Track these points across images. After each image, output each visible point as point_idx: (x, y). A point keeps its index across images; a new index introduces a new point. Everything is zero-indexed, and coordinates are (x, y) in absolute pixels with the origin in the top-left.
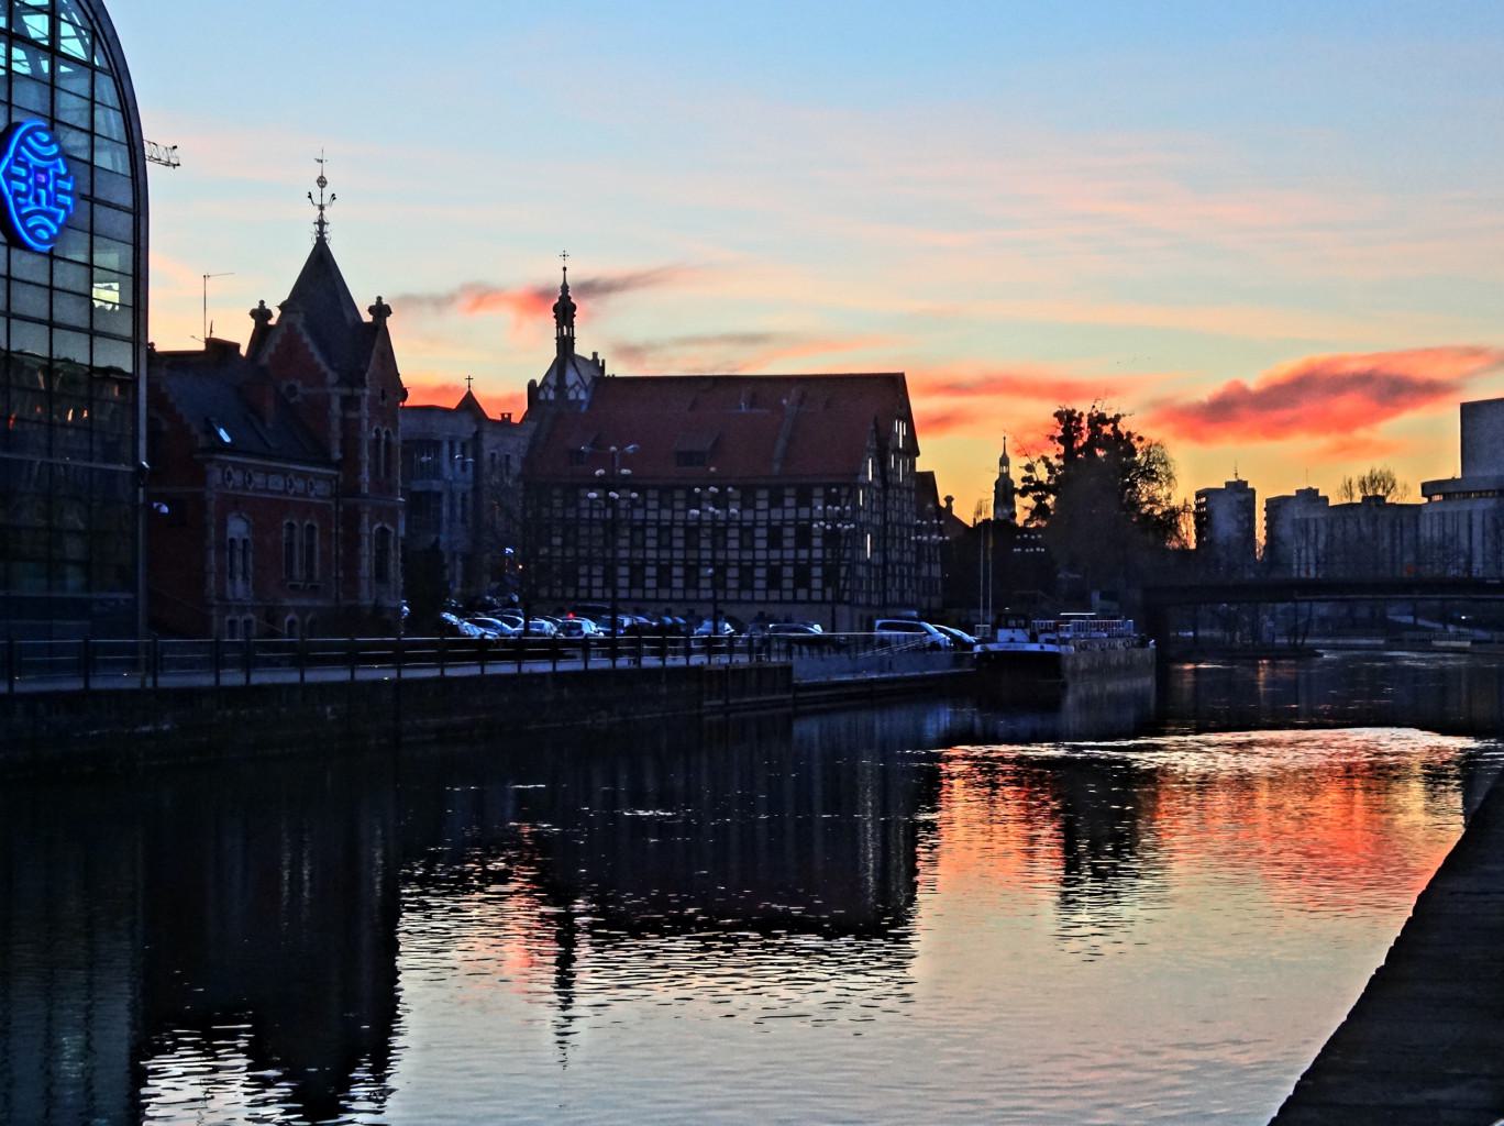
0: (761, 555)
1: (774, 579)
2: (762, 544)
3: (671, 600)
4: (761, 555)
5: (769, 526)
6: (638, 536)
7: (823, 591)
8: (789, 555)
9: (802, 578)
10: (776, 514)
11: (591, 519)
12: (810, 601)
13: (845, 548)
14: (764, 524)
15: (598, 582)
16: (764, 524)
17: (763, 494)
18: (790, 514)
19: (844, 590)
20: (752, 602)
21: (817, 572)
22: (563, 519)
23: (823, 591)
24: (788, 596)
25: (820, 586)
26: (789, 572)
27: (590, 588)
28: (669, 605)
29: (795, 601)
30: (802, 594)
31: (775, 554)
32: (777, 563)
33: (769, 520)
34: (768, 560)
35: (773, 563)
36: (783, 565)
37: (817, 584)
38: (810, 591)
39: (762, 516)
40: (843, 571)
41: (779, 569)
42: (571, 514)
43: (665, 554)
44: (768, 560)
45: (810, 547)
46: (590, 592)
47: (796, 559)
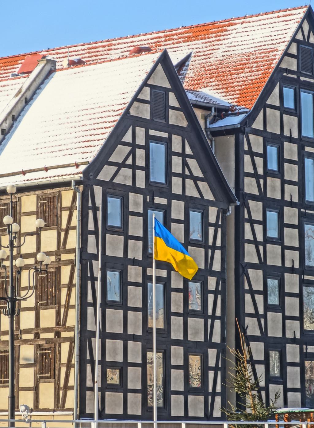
7: (36, 389)
13: (68, 306)
19: (67, 388)
25: (31, 384)
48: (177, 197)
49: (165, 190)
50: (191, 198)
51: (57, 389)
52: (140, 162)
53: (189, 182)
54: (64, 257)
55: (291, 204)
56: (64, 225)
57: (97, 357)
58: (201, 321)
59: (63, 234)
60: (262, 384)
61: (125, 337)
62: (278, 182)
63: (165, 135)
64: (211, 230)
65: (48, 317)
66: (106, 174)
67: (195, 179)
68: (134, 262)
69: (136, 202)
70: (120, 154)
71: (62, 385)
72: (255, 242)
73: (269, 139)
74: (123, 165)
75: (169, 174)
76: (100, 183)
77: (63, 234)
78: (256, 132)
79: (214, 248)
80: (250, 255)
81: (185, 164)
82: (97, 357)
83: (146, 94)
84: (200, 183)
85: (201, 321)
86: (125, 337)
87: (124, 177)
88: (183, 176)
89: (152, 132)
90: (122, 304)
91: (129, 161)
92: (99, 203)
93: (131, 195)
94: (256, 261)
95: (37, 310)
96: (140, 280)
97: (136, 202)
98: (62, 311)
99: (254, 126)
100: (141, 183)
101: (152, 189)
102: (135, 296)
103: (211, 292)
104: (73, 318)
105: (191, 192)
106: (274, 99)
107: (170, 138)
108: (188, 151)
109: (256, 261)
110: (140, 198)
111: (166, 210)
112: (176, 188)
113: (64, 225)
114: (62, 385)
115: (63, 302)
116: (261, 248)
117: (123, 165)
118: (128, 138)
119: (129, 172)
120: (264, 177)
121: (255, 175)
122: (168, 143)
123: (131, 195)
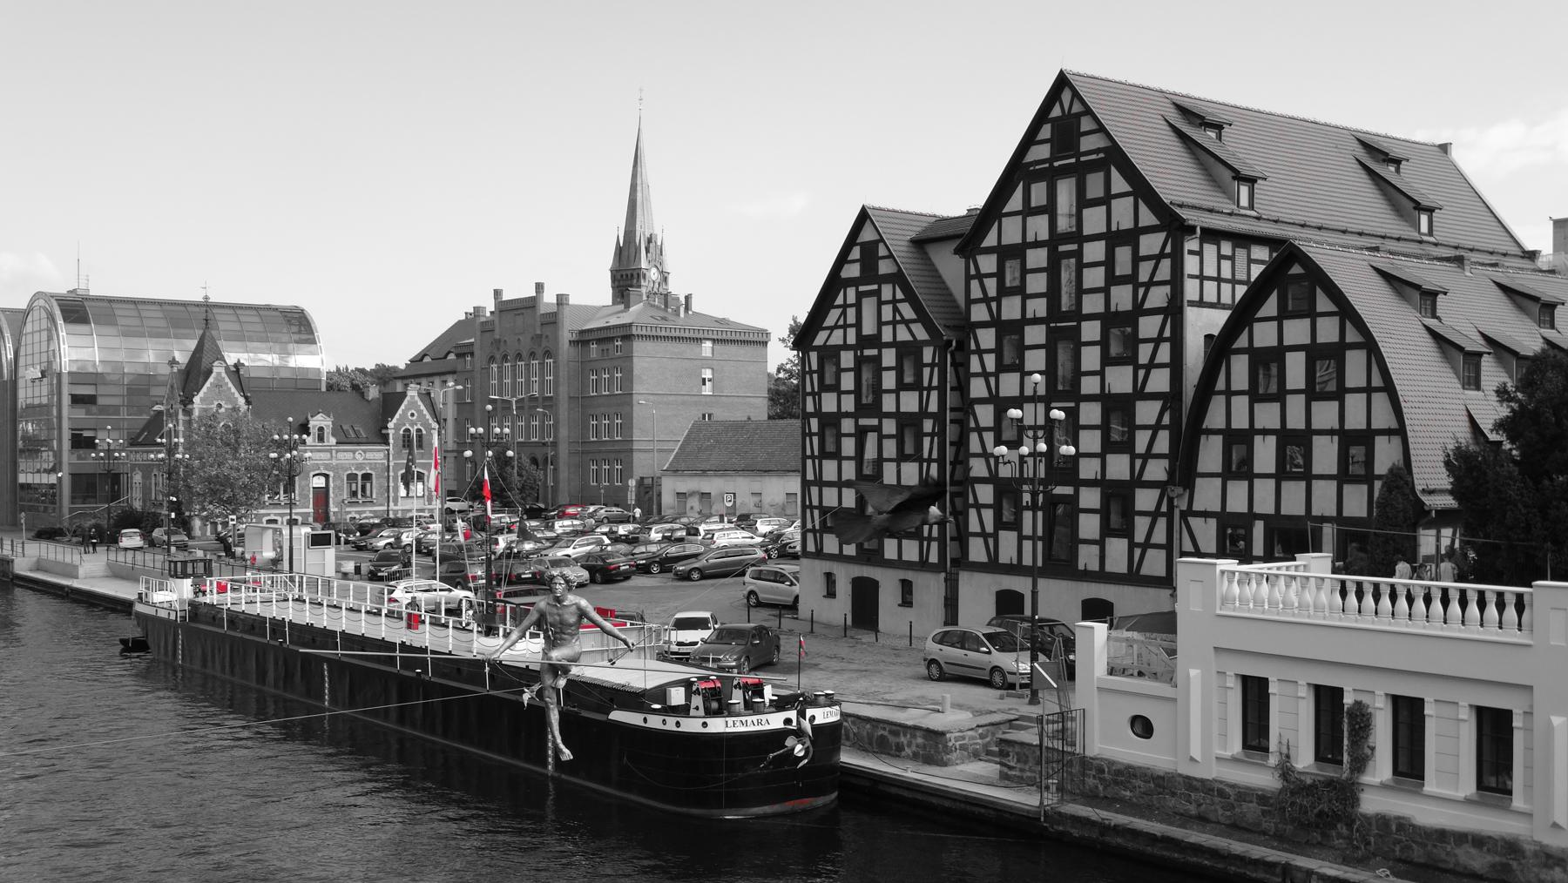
48: (888, 345)
49: (875, 341)
50: (904, 343)
52: (851, 319)
53: (901, 329)
55: (1036, 321)
57: (815, 502)
58: (916, 465)
60: (989, 528)
61: (840, 484)
62: (1017, 300)
63: (875, 287)
64: (926, 371)
66: (820, 340)
67: (907, 323)
68: (847, 415)
69: (847, 359)
70: (832, 317)
72: (985, 374)
73: (1006, 253)
74: (836, 327)
75: (880, 324)
76: (817, 348)
78: (989, 251)
79: (930, 388)
80: (978, 388)
81: (896, 310)
82: (815, 502)
83: (856, 253)
84: (913, 326)
85: (916, 465)
86: (840, 484)
87: (837, 338)
88: (894, 323)
89: (862, 288)
90: (837, 455)
91: (841, 322)
92: (815, 367)
93: (843, 353)
94: (985, 394)
96: (853, 431)
97: (847, 359)
99: (985, 244)
100: (852, 339)
101: (864, 341)
102: (848, 446)
103: (927, 435)
105: (903, 335)
106: (1015, 202)
107: (879, 290)
108: (900, 295)
109: (985, 394)
110: (851, 354)
111: (878, 358)
112: (887, 336)
116: (992, 380)
117: (836, 327)
118: (839, 301)
119: (841, 331)
120: (998, 299)
121: (986, 300)
122: (878, 293)
123: (843, 353)
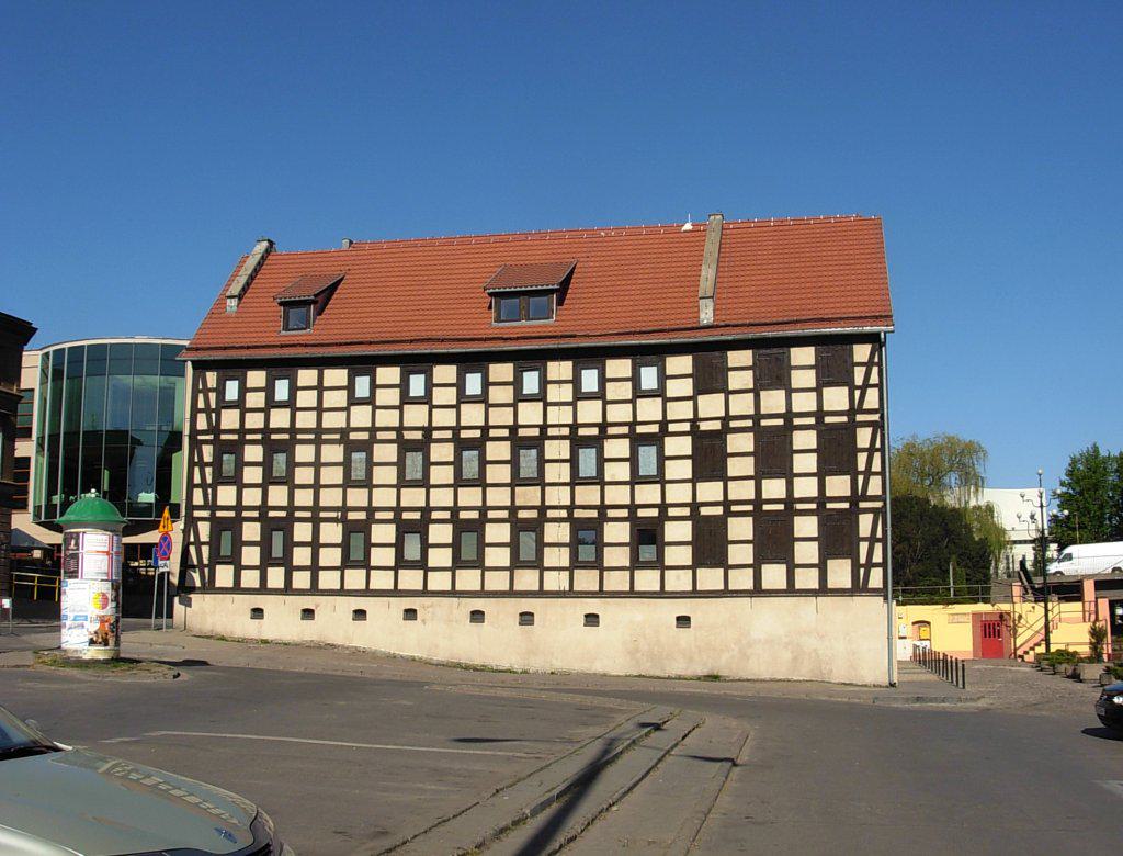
0: (679, 494)
1: (710, 545)
2: (681, 469)
3: (483, 593)
4: (679, 494)
5: (695, 433)
6: (414, 460)
7: (822, 567)
8: (743, 491)
9: (774, 540)
10: (711, 405)
11: (319, 430)
12: (791, 590)
13: (868, 473)
14: (686, 427)
15: (330, 557)
16: (686, 427)
17: (681, 364)
18: (742, 405)
19: (870, 565)
20: (662, 594)
21: (806, 526)
22: (266, 431)
23: (822, 567)
24: (742, 580)
26: (740, 528)
27: (315, 568)
28: (478, 604)
29: (758, 591)
30: (774, 575)
31: (710, 491)
32: (719, 511)
33: (695, 421)
34: (695, 506)
35: (704, 511)
36: (728, 513)
37: (806, 552)
38: (792, 568)
39: (682, 411)
40: (865, 523)
41: (719, 524)
42: (280, 419)
43: (470, 497)
44: (695, 506)
45: (790, 476)
46: (315, 580)
47: (758, 501)
51: (856, 567)
54: (860, 418)
56: (859, 381)
59: (857, 393)
65: (838, 485)
71: (863, 560)
77: (857, 393)
95: (821, 475)
98: (861, 479)
104: (875, 486)
113: (859, 381)
114: (863, 560)
115: (861, 466)
